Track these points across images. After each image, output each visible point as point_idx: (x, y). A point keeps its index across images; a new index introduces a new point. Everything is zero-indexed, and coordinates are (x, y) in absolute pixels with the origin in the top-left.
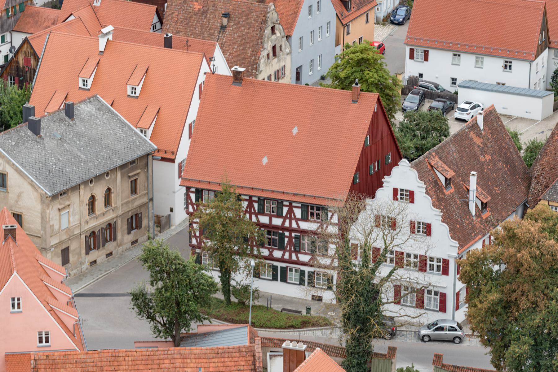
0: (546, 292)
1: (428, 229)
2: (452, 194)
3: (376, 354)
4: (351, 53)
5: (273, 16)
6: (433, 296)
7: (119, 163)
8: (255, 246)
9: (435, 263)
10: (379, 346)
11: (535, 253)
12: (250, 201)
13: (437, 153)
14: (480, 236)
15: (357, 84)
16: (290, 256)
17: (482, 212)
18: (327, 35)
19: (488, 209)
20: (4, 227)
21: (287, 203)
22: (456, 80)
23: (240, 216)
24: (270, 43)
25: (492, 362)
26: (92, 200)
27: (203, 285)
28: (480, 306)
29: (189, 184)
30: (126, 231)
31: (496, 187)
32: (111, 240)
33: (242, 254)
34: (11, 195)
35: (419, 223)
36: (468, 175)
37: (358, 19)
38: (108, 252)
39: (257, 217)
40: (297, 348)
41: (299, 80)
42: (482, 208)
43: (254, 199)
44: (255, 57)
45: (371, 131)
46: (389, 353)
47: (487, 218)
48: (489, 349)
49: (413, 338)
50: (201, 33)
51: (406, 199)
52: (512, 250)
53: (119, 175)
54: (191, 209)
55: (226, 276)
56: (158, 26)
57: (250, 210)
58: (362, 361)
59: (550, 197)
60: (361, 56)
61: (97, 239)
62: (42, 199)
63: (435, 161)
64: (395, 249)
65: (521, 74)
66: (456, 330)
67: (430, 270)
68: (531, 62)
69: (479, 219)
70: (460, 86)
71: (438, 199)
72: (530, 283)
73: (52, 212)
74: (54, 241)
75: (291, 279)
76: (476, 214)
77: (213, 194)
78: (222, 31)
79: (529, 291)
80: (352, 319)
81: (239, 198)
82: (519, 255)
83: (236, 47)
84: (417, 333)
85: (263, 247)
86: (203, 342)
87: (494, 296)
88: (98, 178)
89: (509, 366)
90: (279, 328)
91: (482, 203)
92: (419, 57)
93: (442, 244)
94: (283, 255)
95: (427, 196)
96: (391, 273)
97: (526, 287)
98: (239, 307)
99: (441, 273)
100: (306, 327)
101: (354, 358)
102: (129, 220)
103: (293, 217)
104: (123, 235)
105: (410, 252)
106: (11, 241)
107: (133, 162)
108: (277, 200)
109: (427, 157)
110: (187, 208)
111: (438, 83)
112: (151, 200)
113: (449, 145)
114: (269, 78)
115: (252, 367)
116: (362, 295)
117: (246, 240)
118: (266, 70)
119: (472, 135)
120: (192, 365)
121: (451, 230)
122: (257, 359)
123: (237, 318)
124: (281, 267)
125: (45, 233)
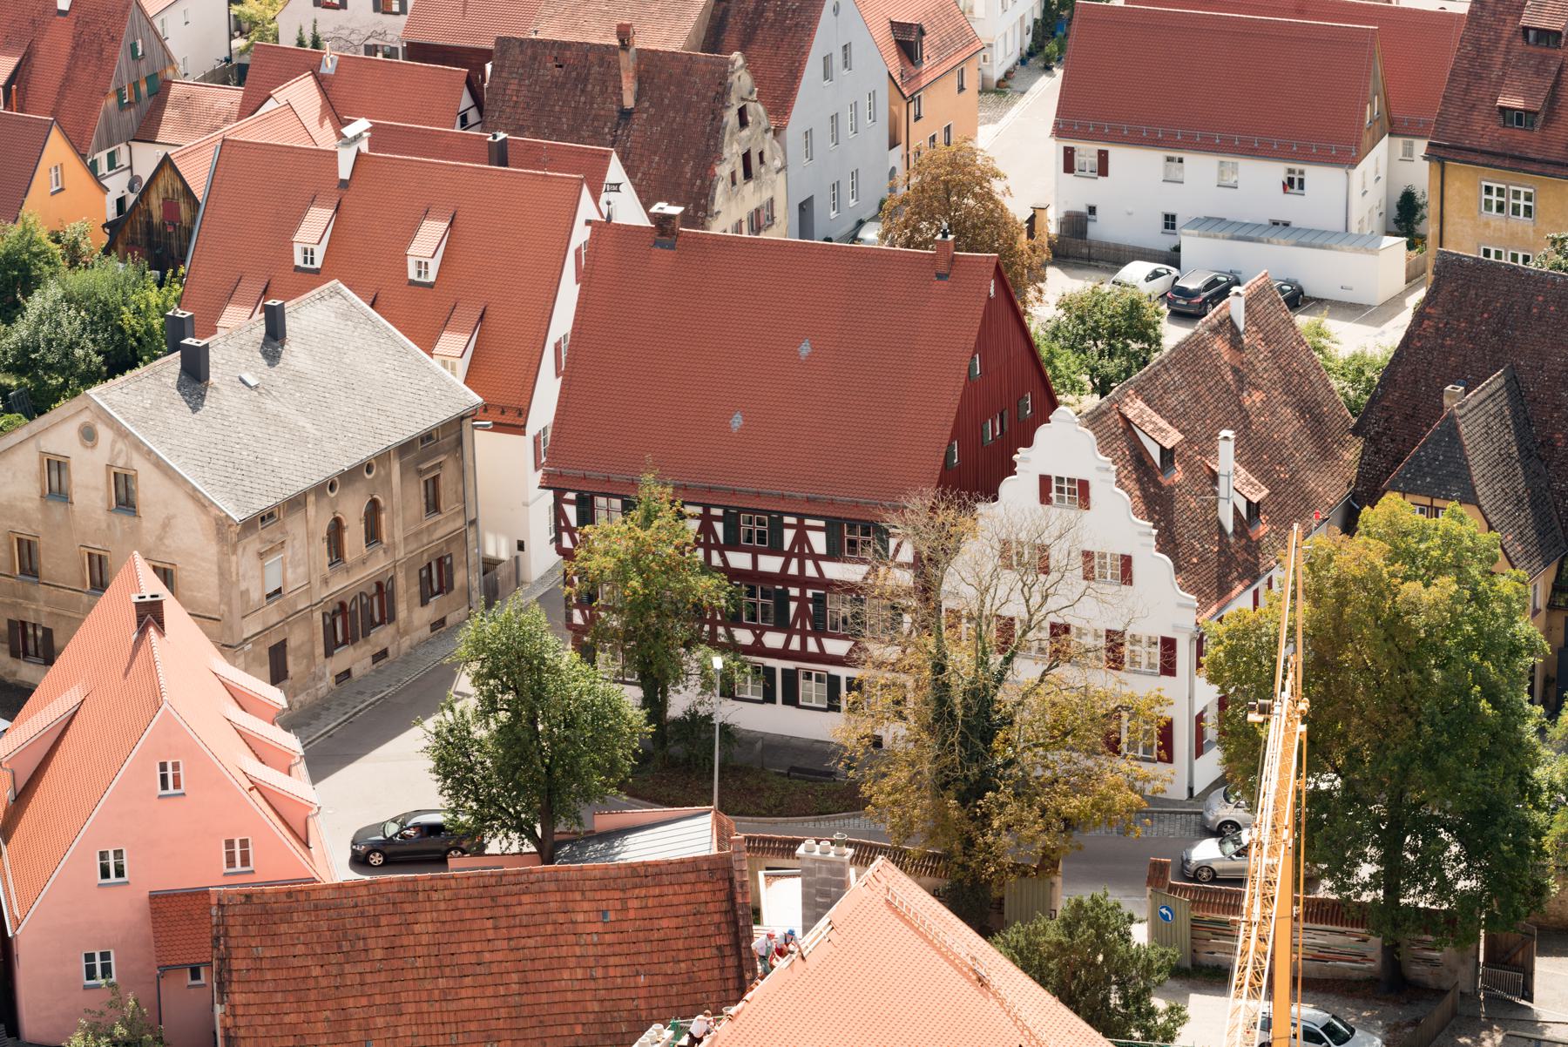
5: (741, 81)
8: (720, 623)
16: (804, 643)
17: (1250, 525)
24: (736, 147)
26: (336, 530)
30: (417, 600)
32: (382, 622)
36: (1212, 438)
37: (940, 83)
38: (378, 650)
45: (981, 346)
53: (396, 468)
54: (567, 542)
56: (473, 116)
59: (1406, 485)
69: (1244, 541)
71: (1145, 497)
73: (245, 561)
74: (251, 627)
76: (1235, 531)
88: (349, 477)
93: (1161, 602)
94: (788, 641)
96: (1044, 674)
102: (424, 573)
104: (410, 610)
108: (768, 512)
110: (558, 540)
112: (473, 522)
113: (1167, 370)
114: (738, 227)
115: (725, 906)
121: (1178, 569)
124: (784, 671)
125: (230, 612)
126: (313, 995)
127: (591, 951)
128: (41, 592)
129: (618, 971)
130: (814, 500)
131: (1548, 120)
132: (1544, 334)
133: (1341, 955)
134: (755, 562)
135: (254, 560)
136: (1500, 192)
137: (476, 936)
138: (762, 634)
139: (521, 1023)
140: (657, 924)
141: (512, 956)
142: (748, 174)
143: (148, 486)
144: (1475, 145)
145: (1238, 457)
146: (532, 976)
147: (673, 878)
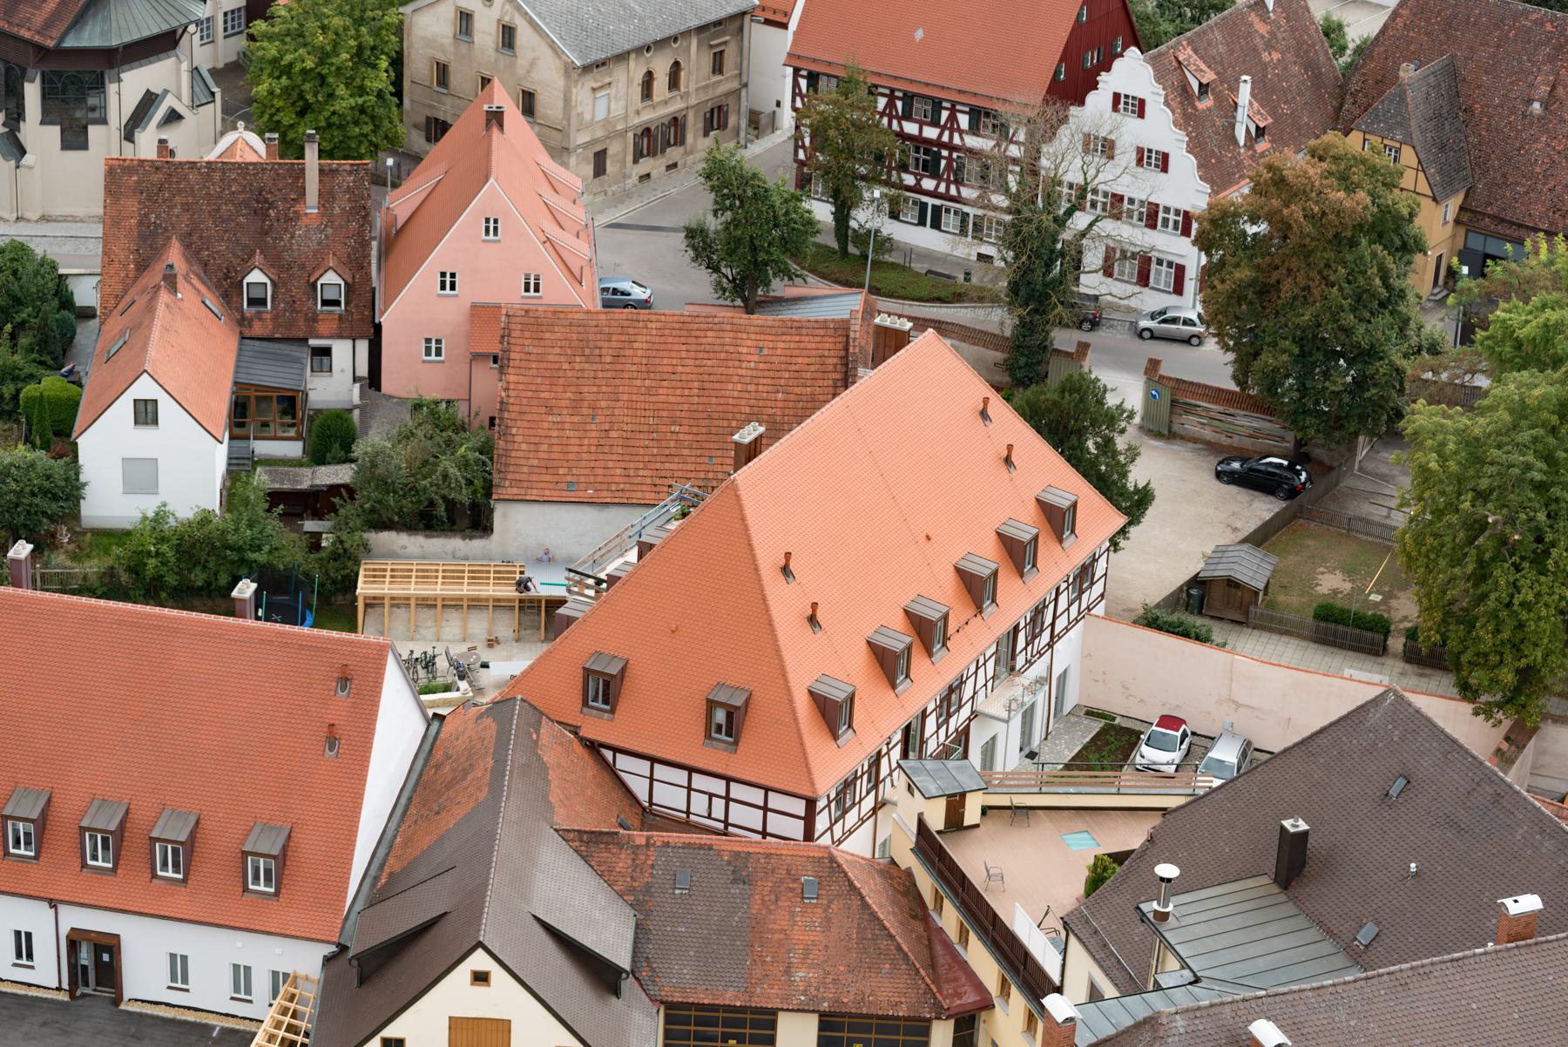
1: (1164, 163)
2: (1209, 109)
6: (1164, 268)
7: (695, 23)
9: (1172, 217)
10: (1064, 339)
13: (1190, 42)
16: (948, 188)
20: (486, 107)
25: (1234, 377)
26: (649, 77)
28: (1219, 287)
29: (798, 64)
33: (872, 180)
34: (520, 61)
35: (1150, 151)
36: (1237, 81)
40: (897, 326)
42: (1258, 136)
43: (898, 94)
48: (1231, 356)
53: (694, 42)
54: (799, 104)
61: (650, 141)
62: (566, 71)
63: (1186, 54)
64: (1102, 187)
66: (1194, 325)
74: (583, 138)
75: (947, 225)
77: (834, 81)
80: (1023, 292)
81: (873, 91)
82: (1285, 212)
84: (1134, 325)
85: (907, 171)
87: (1244, 274)
88: (661, 44)
93: (1185, 188)
94: (937, 186)
96: (1091, 225)
97: (1294, 263)
98: (854, 259)
100: (959, 301)
101: (1022, 354)
104: (695, 138)
106: (495, 131)
107: (718, 23)
108: (932, 98)
110: (794, 101)
112: (746, 85)
115: (843, 353)
116: (1038, 256)
117: (879, 158)
119: (1253, 17)
120: (749, 343)
121: (1200, 166)
123: (854, 280)
126: (561, 381)
127: (750, 373)
128: (449, 101)
129: (765, 389)
133: (1269, 436)
135: (589, 94)
137: (674, 354)
139: (697, 415)
140: (794, 360)
141: (695, 370)
143: (524, 35)
145: (1253, 95)
146: (707, 385)
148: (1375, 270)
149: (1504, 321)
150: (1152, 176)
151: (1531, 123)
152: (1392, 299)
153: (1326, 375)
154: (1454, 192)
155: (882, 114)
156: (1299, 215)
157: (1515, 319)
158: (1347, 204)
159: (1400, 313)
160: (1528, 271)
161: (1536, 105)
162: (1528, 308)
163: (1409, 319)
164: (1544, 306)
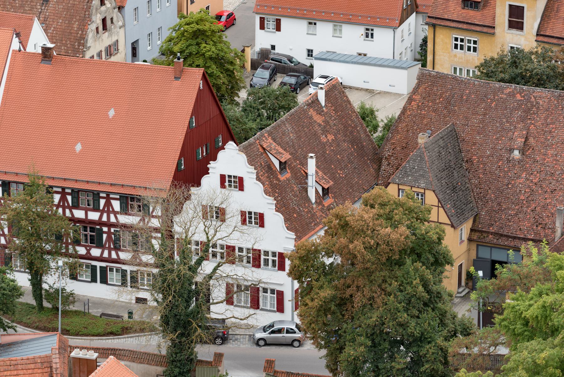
0: (383, 286)
1: (260, 220)
2: (288, 179)
3: (201, 362)
4: (185, 25)
6: (269, 294)
8: (70, 244)
9: (270, 258)
10: (204, 352)
11: (369, 243)
12: (63, 194)
13: (270, 134)
14: (321, 226)
15: (179, 59)
16: (110, 254)
17: (324, 199)
18: (168, 4)
19: (330, 195)
21: (104, 195)
22: (312, 51)
23: (52, 211)
24: (99, 15)
25: (328, 366)
27: (4, 290)
28: (310, 304)
31: (340, 170)
33: (55, 253)
35: (250, 213)
39: (71, 212)
41: (136, 56)
42: (324, 194)
44: (82, 32)
45: (196, 111)
46: (215, 360)
47: (329, 206)
48: (324, 352)
49: (247, 342)
50: (22, 6)
51: (235, 187)
52: (343, 240)
55: (37, 278)
57: (64, 204)
58: (185, 370)
59: (399, 180)
60: (195, 27)
63: (268, 143)
65: (384, 42)
66: (295, 333)
67: (264, 265)
68: (395, 29)
69: (320, 207)
70: (316, 59)
71: (271, 185)
72: (366, 277)
75: (112, 279)
77: (21, 187)
78: (45, 3)
79: (364, 286)
80: (171, 323)
81: (49, 190)
82: (351, 246)
83: (61, 21)
84: (252, 337)
85: (79, 245)
86: (7, 354)
87: (327, 293)
89: (345, 370)
90: (96, 336)
91: (323, 189)
92: (271, 27)
93: (277, 236)
94: (102, 253)
95: (258, 182)
96: (215, 269)
99: (277, 268)
100: (127, 333)
103: (111, 210)
105: (241, 246)
108: (92, 192)
109: (258, 139)
111: (292, 55)
114: (99, 54)
116: (181, 296)
117: (59, 237)
118: (96, 45)
119: (312, 112)
121: (286, 220)
122: (54, 370)
123: (50, 326)
124: (101, 267)
130: (115, 185)
131: (485, 6)
132: (469, 109)
134: (86, 215)
136: (462, 40)
138: (90, 249)
142: (105, 28)
144: (450, 18)
145: (318, 166)
147: (23, 367)
148: (418, 280)
149: (513, 307)
150: (254, 230)
151: (514, 166)
152: (433, 299)
153: (392, 358)
154: (466, 220)
155: (58, 206)
156: (361, 247)
157: (522, 305)
158: (394, 236)
159: (440, 309)
160: (525, 270)
161: (516, 153)
162: (530, 296)
163: (446, 312)
164: (540, 295)
